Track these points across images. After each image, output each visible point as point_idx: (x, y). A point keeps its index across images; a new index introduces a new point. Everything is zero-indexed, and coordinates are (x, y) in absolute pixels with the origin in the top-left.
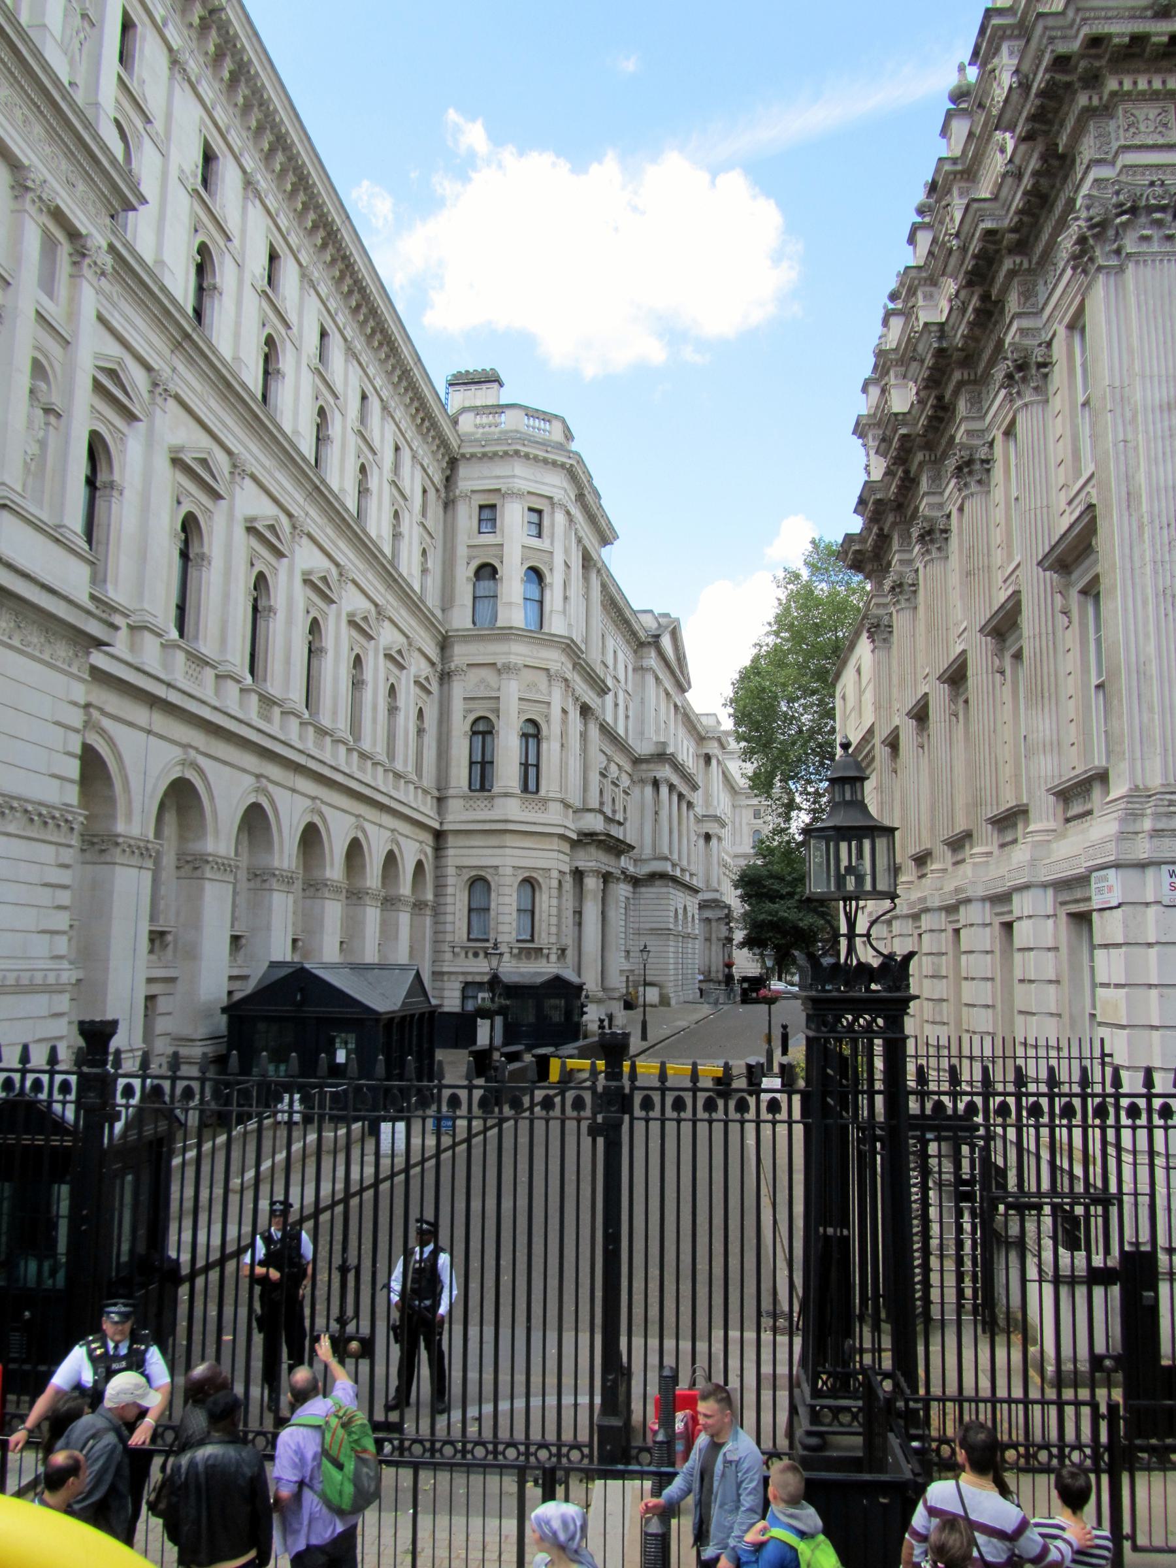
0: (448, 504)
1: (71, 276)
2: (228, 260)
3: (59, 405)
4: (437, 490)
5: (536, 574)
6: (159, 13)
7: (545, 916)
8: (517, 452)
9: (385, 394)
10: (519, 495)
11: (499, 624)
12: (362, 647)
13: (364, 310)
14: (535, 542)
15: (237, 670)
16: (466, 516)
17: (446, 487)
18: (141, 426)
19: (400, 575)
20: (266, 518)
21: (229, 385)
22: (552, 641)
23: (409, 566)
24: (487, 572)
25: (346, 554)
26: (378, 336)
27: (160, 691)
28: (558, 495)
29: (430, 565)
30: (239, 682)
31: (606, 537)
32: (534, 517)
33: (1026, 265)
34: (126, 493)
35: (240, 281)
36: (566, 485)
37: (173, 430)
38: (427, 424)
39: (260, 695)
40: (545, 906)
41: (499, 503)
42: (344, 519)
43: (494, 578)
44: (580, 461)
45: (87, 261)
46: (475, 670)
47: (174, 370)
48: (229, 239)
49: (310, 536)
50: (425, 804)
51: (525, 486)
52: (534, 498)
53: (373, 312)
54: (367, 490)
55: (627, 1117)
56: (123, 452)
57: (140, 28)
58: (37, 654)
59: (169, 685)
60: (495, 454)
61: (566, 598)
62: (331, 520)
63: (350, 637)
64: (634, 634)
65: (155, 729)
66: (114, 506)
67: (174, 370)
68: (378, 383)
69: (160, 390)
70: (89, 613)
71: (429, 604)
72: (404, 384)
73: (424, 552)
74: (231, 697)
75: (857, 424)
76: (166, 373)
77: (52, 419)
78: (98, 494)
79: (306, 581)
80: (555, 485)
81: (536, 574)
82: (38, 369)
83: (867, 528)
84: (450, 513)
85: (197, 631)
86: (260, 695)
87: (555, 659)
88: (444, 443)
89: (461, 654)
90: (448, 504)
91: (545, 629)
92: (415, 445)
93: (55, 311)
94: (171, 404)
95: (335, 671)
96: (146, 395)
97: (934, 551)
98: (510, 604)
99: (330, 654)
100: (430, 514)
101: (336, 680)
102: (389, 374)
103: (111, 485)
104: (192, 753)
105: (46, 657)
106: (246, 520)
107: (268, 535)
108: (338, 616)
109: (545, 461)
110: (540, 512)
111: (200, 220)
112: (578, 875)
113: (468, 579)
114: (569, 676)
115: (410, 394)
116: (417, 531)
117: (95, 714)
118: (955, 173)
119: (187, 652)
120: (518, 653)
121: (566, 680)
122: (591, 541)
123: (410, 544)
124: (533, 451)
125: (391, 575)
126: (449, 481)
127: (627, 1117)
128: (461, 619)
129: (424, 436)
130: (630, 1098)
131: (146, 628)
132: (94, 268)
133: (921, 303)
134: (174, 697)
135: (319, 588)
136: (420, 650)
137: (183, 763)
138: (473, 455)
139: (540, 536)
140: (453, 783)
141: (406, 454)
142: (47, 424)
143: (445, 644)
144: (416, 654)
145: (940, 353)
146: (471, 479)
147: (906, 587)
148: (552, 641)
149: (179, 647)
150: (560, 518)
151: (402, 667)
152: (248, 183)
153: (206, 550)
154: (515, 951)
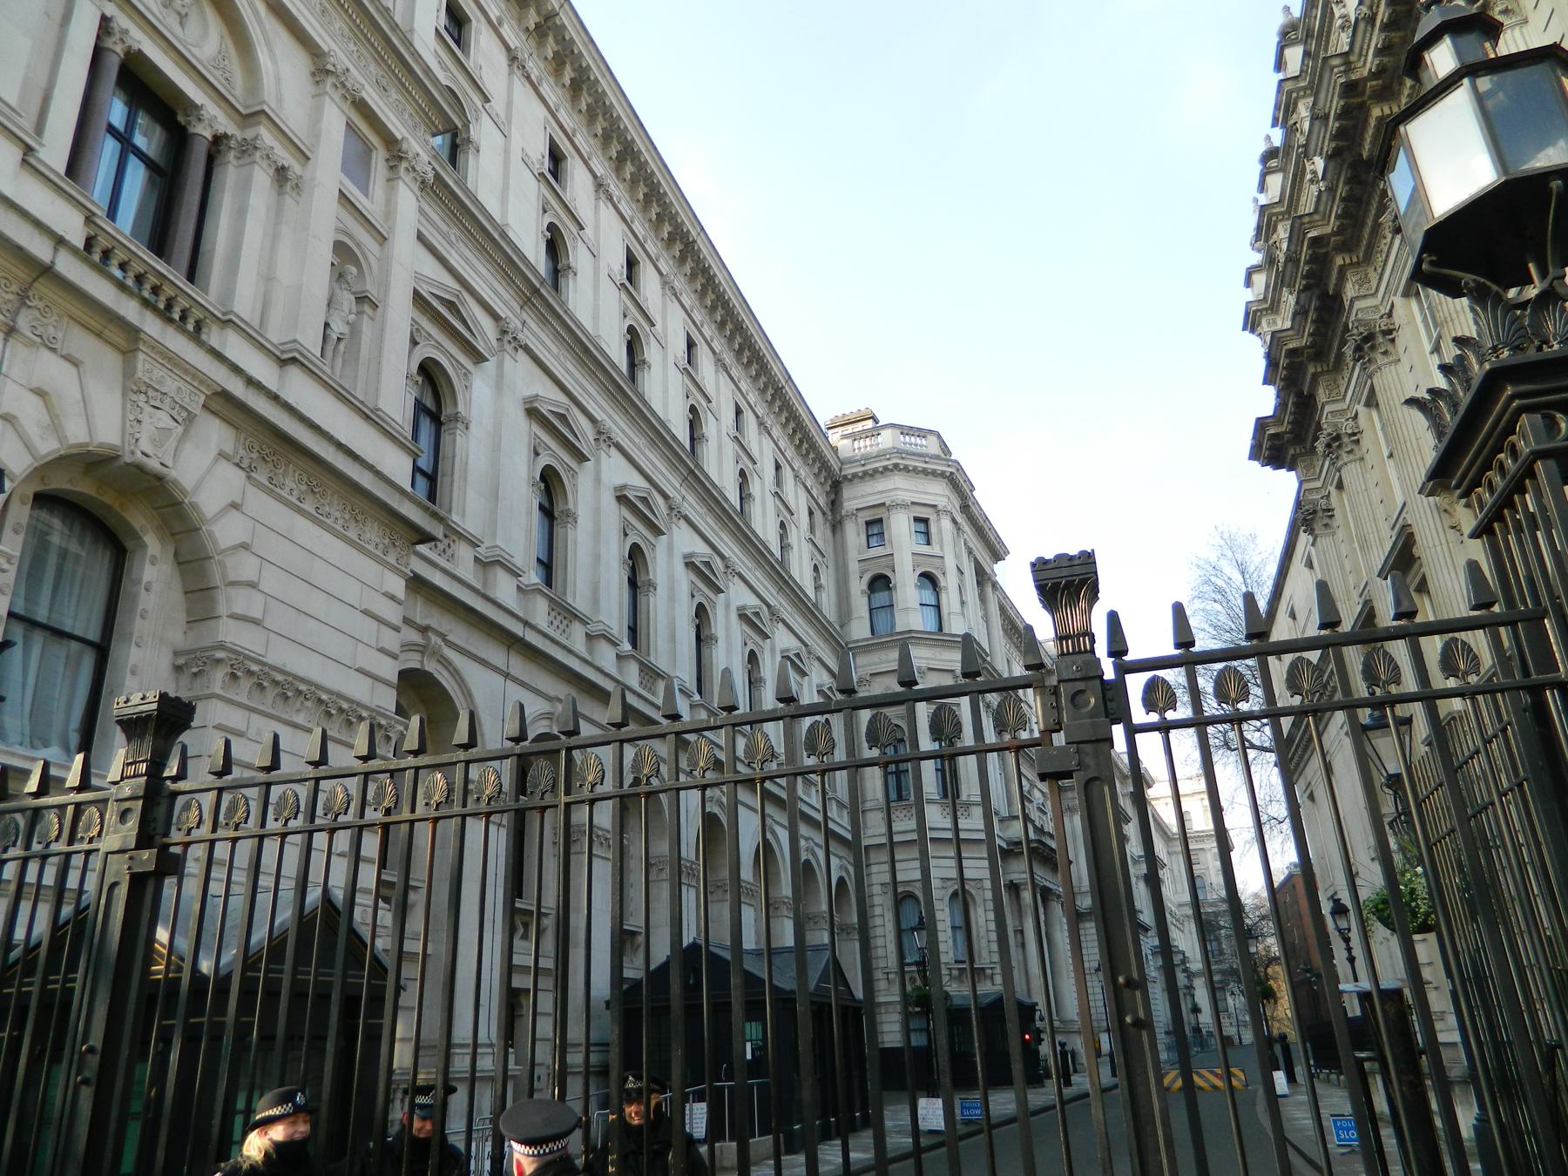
0: (836, 526)
2: (581, 248)
3: (373, 292)
6: (494, 13)
7: (983, 932)
8: (896, 466)
9: (760, 411)
12: (756, 644)
13: (729, 326)
14: (925, 549)
15: (615, 631)
16: (854, 535)
17: (832, 511)
18: (490, 366)
20: (635, 488)
21: (586, 350)
23: (801, 569)
24: (880, 583)
26: (747, 353)
27: (516, 628)
28: (942, 502)
29: (823, 581)
30: (615, 645)
32: (922, 527)
34: (472, 426)
36: (947, 492)
37: (525, 381)
38: (805, 445)
39: (641, 663)
40: (981, 921)
43: (889, 589)
44: (960, 469)
45: (404, 164)
46: (879, 679)
49: (686, 518)
50: (841, 817)
51: (909, 497)
53: (739, 328)
54: (750, 495)
55: (1118, 731)
57: (474, 23)
58: (338, 527)
59: (526, 623)
60: (876, 471)
61: (963, 603)
62: (711, 510)
65: (512, 672)
68: (752, 398)
69: (509, 337)
70: (402, 491)
72: (778, 403)
73: (816, 568)
74: (606, 657)
75: (1247, 314)
76: (515, 323)
77: (367, 308)
79: (687, 564)
80: (938, 493)
81: (929, 579)
82: (343, 251)
83: (1281, 406)
84: (838, 535)
85: (565, 588)
86: (641, 663)
88: (824, 466)
90: (836, 526)
91: (946, 630)
93: (372, 206)
94: (521, 355)
96: (495, 343)
100: (818, 533)
102: (763, 391)
103: (456, 418)
105: (352, 534)
106: (616, 489)
107: (641, 506)
108: (727, 606)
109: (925, 472)
110: (925, 521)
111: (548, 202)
115: (785, 414)
116: (807, 548)
117: (434, 639)
122: (983, 556)
124: (912, 463)
126: (835, 504)
127: (1118, 731)
128: (859, 629)
129: (805, 457)
130: (1119, 687)
132: (412, 174)
134: (532, 638)
135: (700, 571)
136: (819, 659)
138: (855, 475)
140: (869, 795)
141: (787, 474)
142: (360, 313)
144: (816, 663)
145: (1350, 88)
146: (856, 498)
147: (1346, 440)
150: (946, 523)
151: (803, 674)
154: (955, 973)
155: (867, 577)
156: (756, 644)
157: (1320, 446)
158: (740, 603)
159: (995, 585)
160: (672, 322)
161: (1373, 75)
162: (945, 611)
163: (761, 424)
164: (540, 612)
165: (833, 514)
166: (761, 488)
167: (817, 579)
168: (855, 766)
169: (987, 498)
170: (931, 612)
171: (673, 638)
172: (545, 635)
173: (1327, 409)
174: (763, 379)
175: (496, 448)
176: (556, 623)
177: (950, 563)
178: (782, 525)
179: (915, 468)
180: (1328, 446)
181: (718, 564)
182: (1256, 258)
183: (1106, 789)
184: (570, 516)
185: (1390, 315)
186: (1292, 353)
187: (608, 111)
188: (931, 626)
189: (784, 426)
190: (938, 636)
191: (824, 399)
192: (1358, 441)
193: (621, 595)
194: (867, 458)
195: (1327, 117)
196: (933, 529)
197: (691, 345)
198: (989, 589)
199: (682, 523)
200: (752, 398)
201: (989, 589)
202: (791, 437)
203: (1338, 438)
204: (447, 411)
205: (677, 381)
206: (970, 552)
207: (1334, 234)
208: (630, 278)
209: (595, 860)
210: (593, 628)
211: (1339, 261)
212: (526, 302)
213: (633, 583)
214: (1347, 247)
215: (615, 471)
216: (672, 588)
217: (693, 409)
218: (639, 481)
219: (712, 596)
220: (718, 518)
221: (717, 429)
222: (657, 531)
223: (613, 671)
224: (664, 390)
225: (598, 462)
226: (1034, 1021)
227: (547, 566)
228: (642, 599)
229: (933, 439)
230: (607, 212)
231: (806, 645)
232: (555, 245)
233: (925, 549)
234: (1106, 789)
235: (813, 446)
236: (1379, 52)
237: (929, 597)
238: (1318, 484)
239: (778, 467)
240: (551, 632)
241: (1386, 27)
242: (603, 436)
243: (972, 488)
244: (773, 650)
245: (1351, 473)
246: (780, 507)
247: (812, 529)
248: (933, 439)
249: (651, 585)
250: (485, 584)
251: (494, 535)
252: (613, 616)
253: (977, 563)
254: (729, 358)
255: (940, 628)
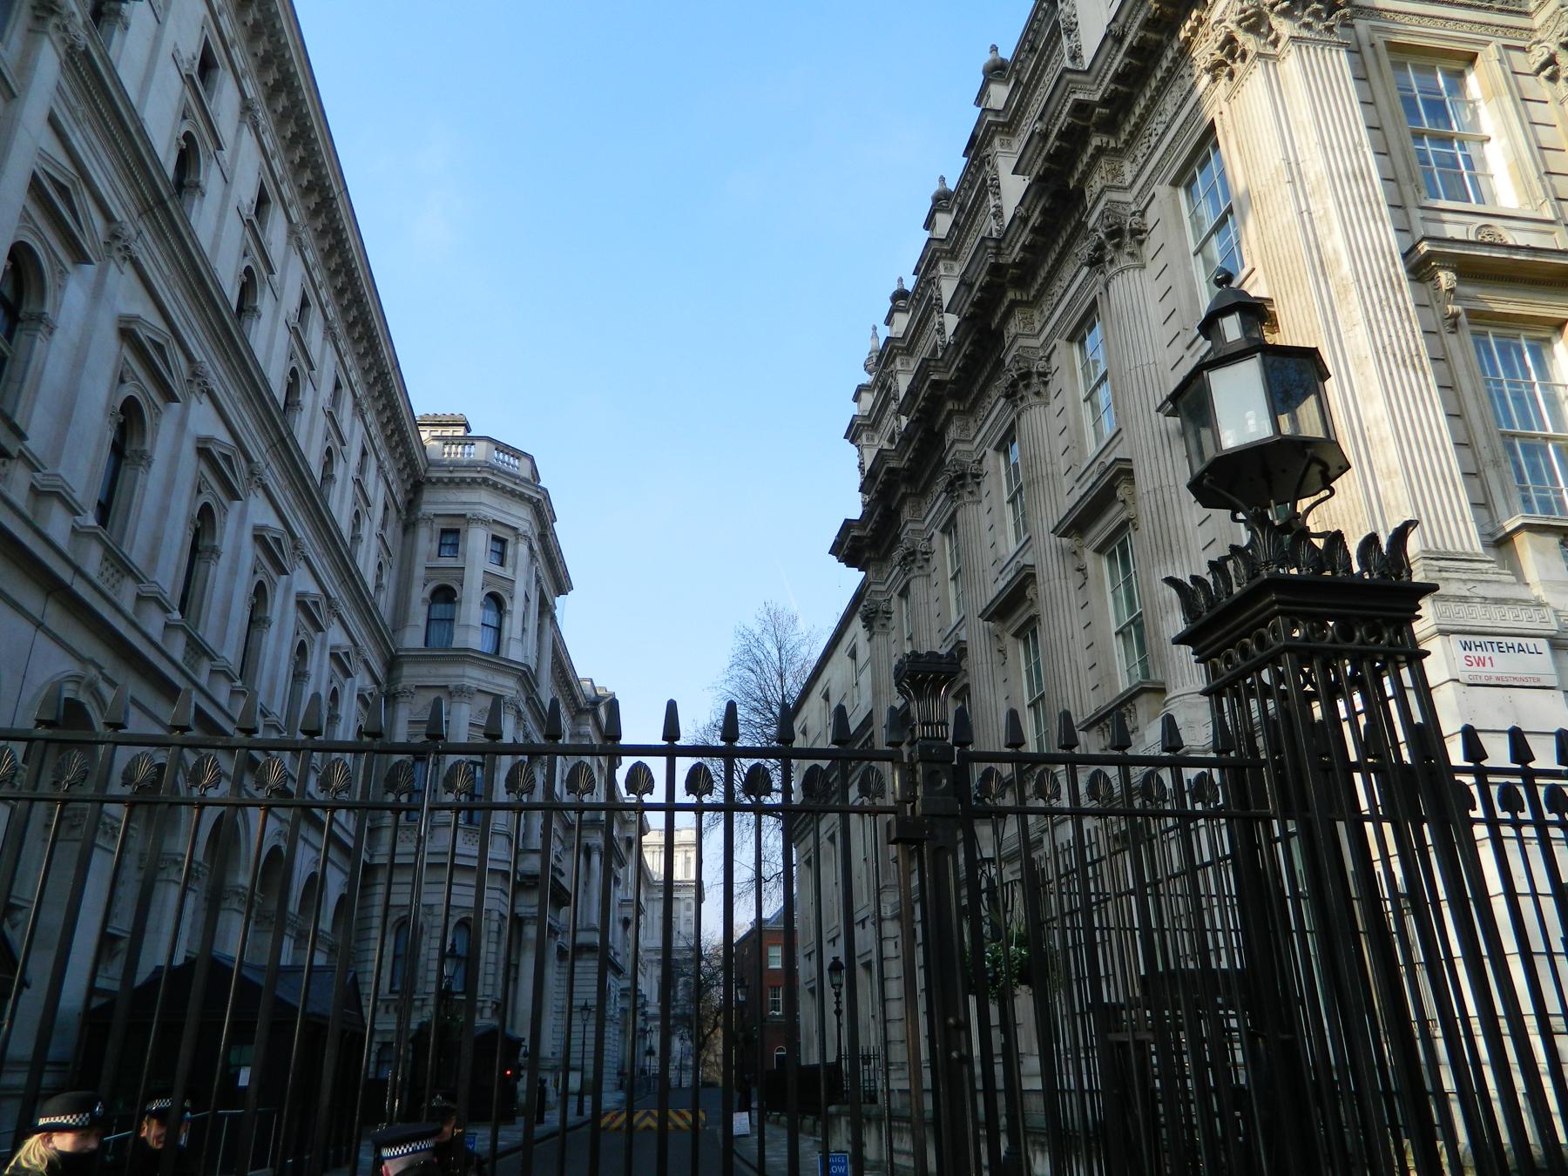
1: (30, 30)
2: (214, 169)
4: (398, 511)
5: (496, 601)
8: (485, 480)
9: (359, 391)
10: (485, 522)
11: (455, 645)
12: (308, 635)
13: (348, 296)
14: (497, 570)
16: (426, 541)
17: (408, 510)
18: (90, 270)
19: (358, 570)
20: (222, 444)
21: (201, 281)
22: (507, 667)
24: (445, 595)
25: (302, 529)
26: (359, 328)
27: (66, 574)
28: (523, 527)
29: (384, 580)
30: (166, 610)
31: (562, 585)
32: (498, 547)
33: (1112, 144)
34: (58, 335)
35: (226, 197)
36: (530, 518)
38: (396, 438)
39: (190, 636)
41: (462, 529)
42: (306, 487)
47: (139, 233)
48: (220, 148)
49: (266, 489)
51: (492, 514)
52: (498, 528)
56: (61, 287)
60: (463, 480)
61: (524, 630)
63: (297, 619)
64: (574, 698)
66: (38, 343)
67: (139, 233)
68: (354, 376)
69: (120, 244)
71: (381, 608)
72: (379, 387)
78: (19, 326)
80: (520, 517)
81: (496, 601)
87: (508, 686)
89: (410, 675)
90: (409, 527)
91: (503, 654)
92: (382, 456)
94: (127, 267)
95: (276, 647)
97: (966, 495)
98: (468, 626)
99: (274, 628)
101: (276, 659)
102: (366, 372)
103: (40, 318)
104: (93, 672)
109: (513, 493)
110: (503, 542)
111: (190, 109)
112: (518, 922)
113: (424, 600)
114: (523, 707)
116: (375, 543)
118: (997, 124)
119: (107, 549)
120: (474, 676)
121: (519, 712)
122: (548, 587)
123: (368, 552)
125: (348, 570)
126: (412, 504)
128: (413, 638)
129: (392, 450)
131: (58, 496)
133: (942, 272)
134: (81, 588)
136: (366, 663)
137: (77, 680)
138: (440, 480)
139: (502, 564)
141: (372, 463)
143: (393, 663)
144: (362, 666)
145: (996, 269)
146: (437, 503)
147: (919, 556)
148: (507, 667)
149: (97, 537)
150: (523, 548)
151: (348, 674)
152: (246, 108)
153: (147, 447)
155: (431, 586)
156: (308, 635)
157: (897, 556)
158: (300, 589)
159: (553, 618)
160: (291, 276)
161: (1015, 265)
162: (505, 634)
163: (357, 404)
164: (93, 559)
165: (408, 514)
166: (344, 471)
167: (379, 577)
168: (670, 808)
169: (565, 532)
170: (490, 633)
171: (226, 615)
172: (96, 588)
173: (909, 526)
174: (370, 359)
175: (78, 364)
176: (106, 575)
177: (520, 588)
178: (357, 514)
179: (504, 487)
180: (904, 558)
181: (287, 543)
182: (867, 379)
183: (950, 858)
184: (144, 458)
185: (980, 462)
186: (890, 471)
187: (275, 34)
188: (488, 647)
189: (379, 413)
190: (494, 659)
191: (426, 394)
192: (927, 560)
193: (180, 558)
194: (456, 465)
195: (971, 286)
196: (510, 552)
197: (305, 303)
198: (547, 621)
199: (260, 492)
200: (354, 376)
201: (547, 621)
202: (384, 426)
203: (913, 553)
204: (29, 307)
205: (283, 337)
206: (538, 581)
207: (951, 382)
208: (257, 213)
209: (329, 865)
210: (146, 589)
211: (949, 406)
212: (146, 211)
213: (194, 549)
214: (959, 396)
215: (202, 420)
216: (236, 559)
217: (294, 373)
218: (223, 435)
219: (273, 574)
220: (298, 494)
221: (314, 399)
222: (233, 495)
223: (157, 638)
224: (269, 341)
225: (186, 408)
226: (517, 1055)
227: (104, 510)
228: (200, 567)
229: (526, 463)
230: (248, 139)
231: (356, 645)
232: (188, 156)
233: (497, 570)
234: (950, 858)
235: (404, 440)
236: (1024, 248)
237: (491, 618)
238: (883, 588)
239: (364, 453)
240: (99, 582)
241: (1034, 230)
242: (196, 376)
243: (554, 519)
244: (323, 644)
245: (917, 586)
246: (357, 493)
247: (384, 526)
248: (526, 463)
249: (215, 552)
250: (35, 514)
251: (57, 461)
252: (167, 576)
253: (542, 591)
254: (339, 328)
255: (497, 651)
